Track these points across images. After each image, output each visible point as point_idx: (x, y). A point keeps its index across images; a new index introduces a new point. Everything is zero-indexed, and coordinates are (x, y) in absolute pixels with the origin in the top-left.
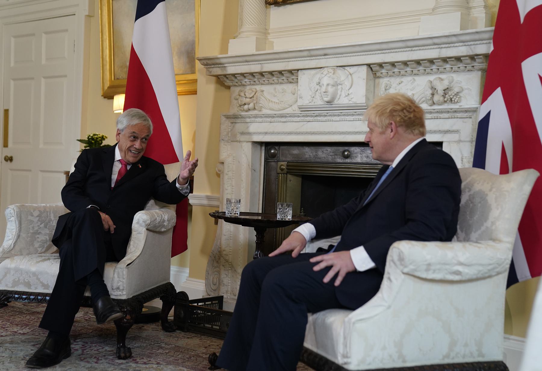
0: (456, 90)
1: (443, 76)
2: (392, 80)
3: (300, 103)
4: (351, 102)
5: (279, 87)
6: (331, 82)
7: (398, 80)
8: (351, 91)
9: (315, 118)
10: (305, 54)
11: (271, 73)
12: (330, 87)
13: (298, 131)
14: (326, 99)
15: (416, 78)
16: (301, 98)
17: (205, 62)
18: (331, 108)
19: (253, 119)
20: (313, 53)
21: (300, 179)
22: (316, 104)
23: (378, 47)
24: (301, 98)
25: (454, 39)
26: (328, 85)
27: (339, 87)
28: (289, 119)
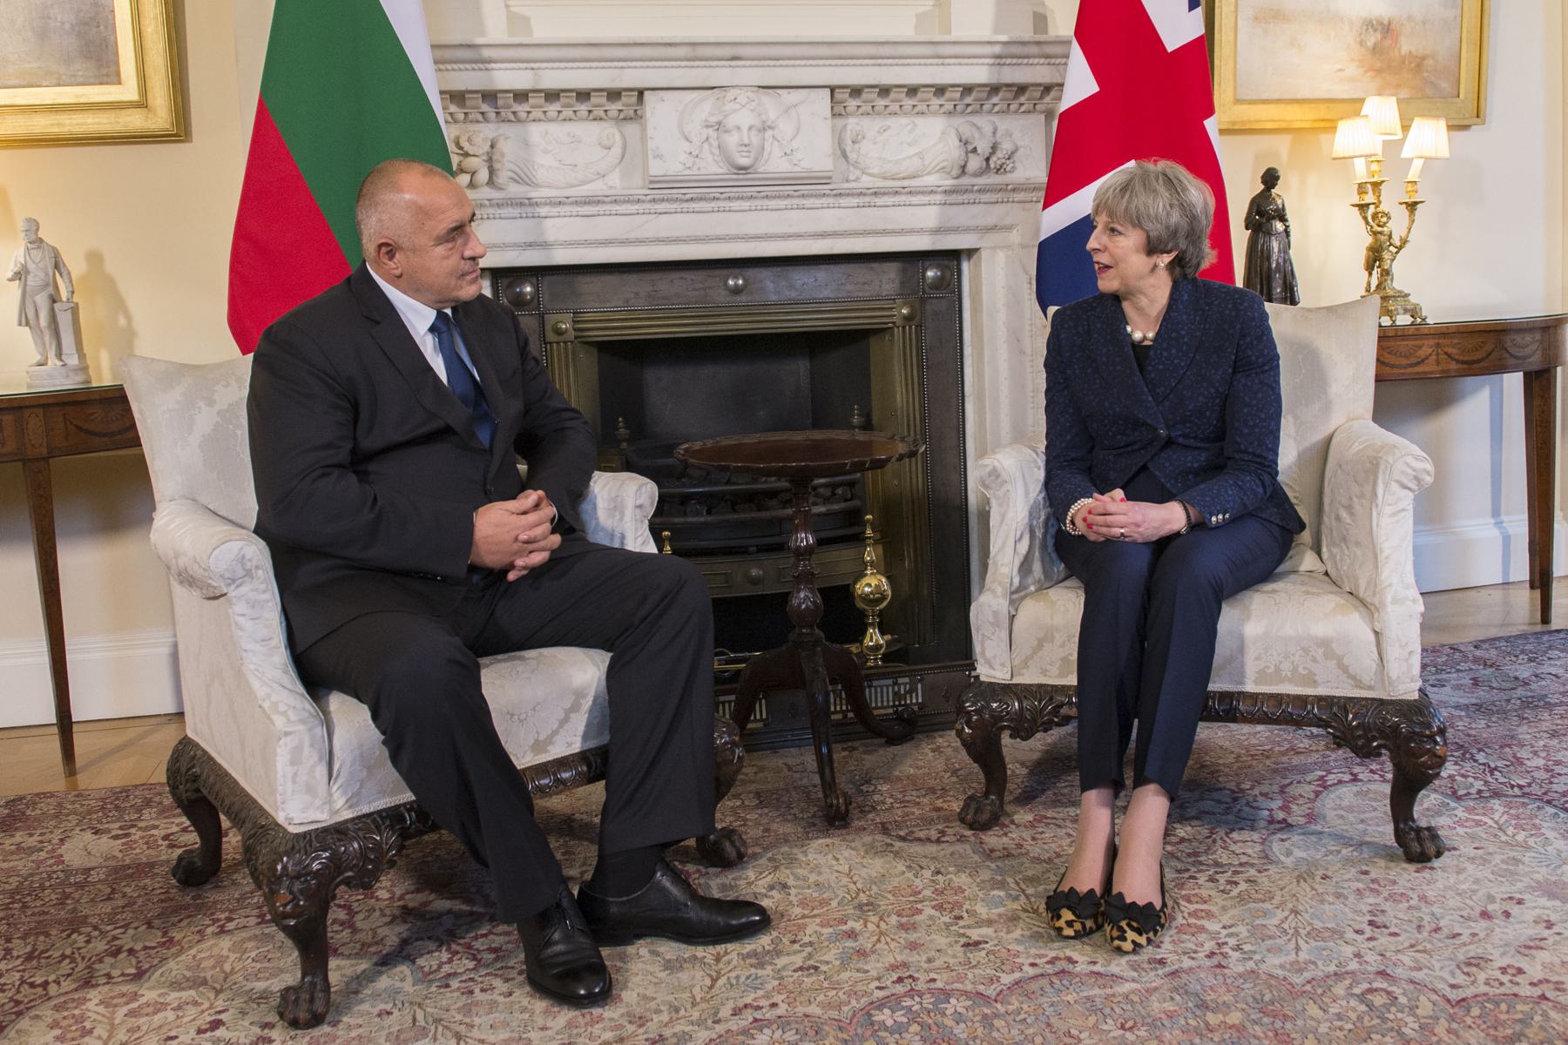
0: (1006, 146)
1: (979, 120)
2: (865, 121)
3: (656, 168)
4: (796, 169)
5: (558, 130)
6: (758, 124)
7: (878, 123)
8: (795, 145)
9: (685, 205)
10: (681, 52)
11: (552, 96)
12: (754, 132)
13: (632, 236)
14: (744, 161)
15: (919, 121)
16: (658, 156)
18: (744, 181)
19: (491, 211)
20: (701, 51)
21: (600, 350)
23: (873, 50)
24: (658, 156)
25: (1034, 50)
26: (750, 128)
27: (769, 133)
28: (607, 207)
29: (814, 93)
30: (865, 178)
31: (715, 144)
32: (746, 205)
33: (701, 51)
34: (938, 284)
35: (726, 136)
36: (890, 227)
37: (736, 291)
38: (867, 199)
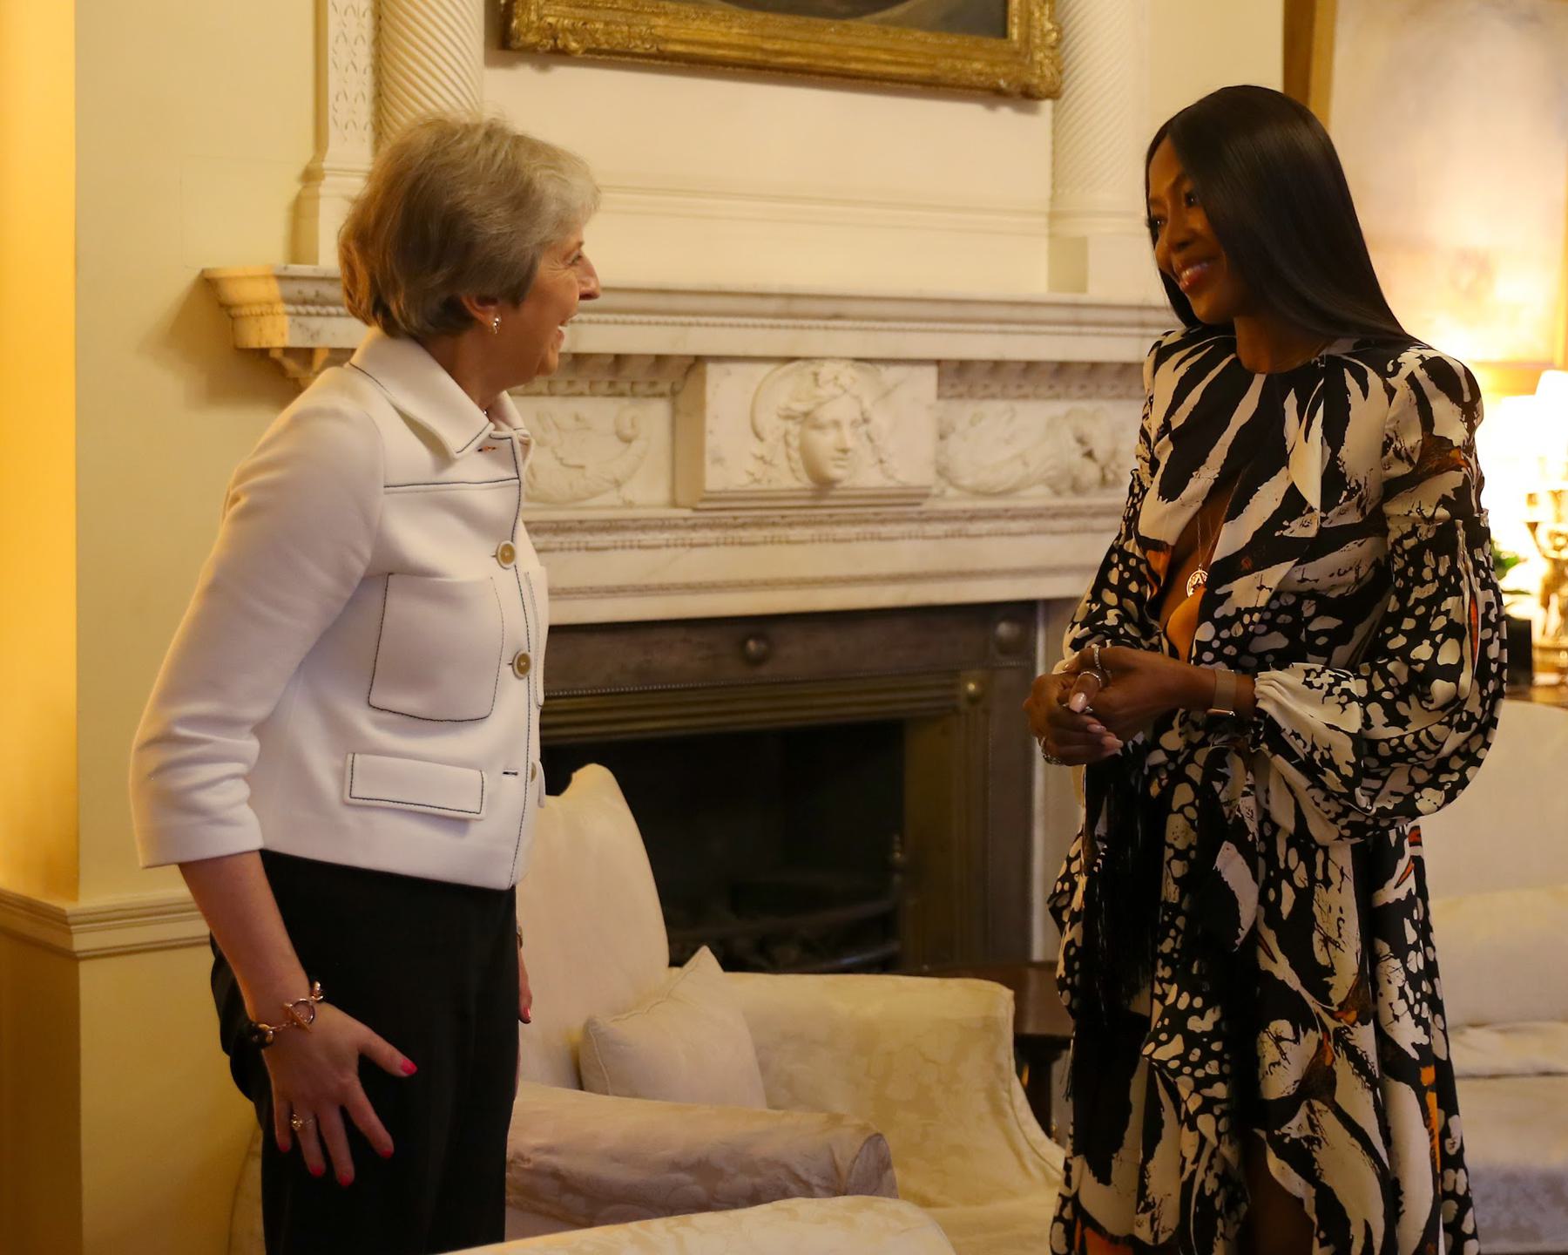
3: (715, 479)
4: (891, 483)
10: (771, 305)
13: (654, 580)
16: (719, 460)
17: (309, 290)
18: (822, 500)
20: (799, 307)
22: (774, 486)
24: (719, 460)
29: (917, 371)
30: (951, 492)
31: (795, 443)
32: (807, 533)
33: (799, 307)
34: (1006, 648)
35: (814, 435)
36: (981, 566)
37: (757, 661)
38: (956, 526)
